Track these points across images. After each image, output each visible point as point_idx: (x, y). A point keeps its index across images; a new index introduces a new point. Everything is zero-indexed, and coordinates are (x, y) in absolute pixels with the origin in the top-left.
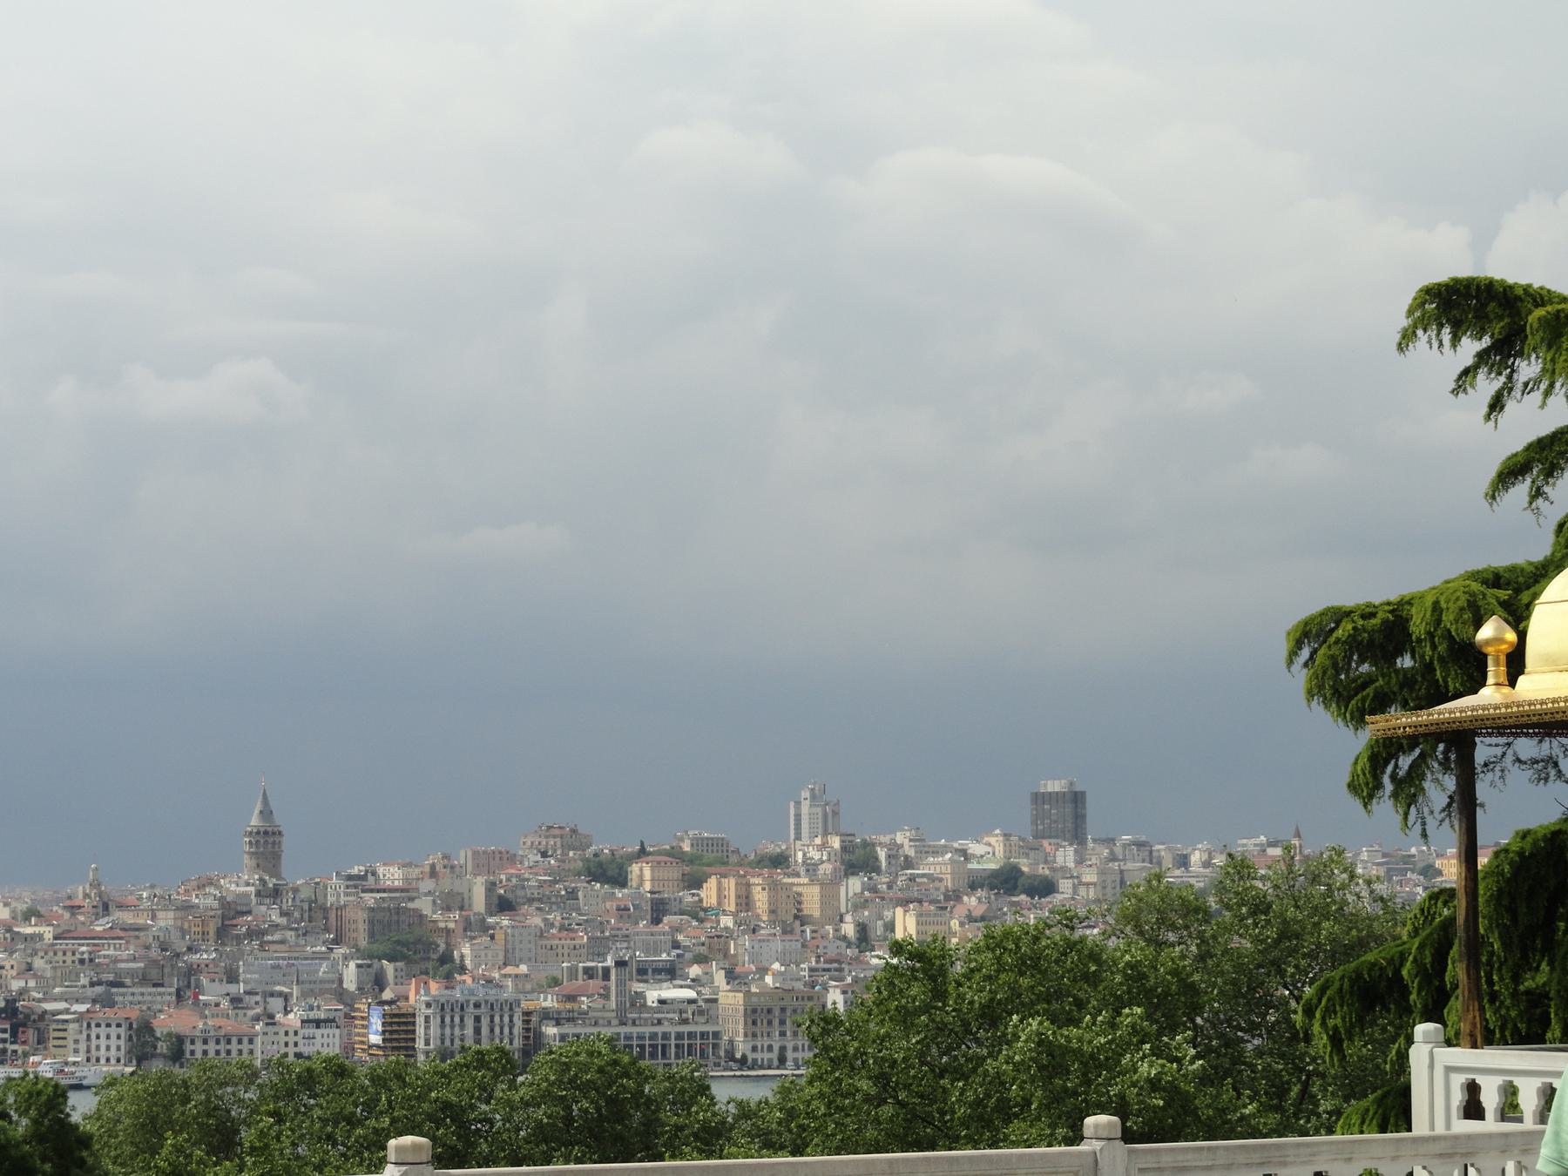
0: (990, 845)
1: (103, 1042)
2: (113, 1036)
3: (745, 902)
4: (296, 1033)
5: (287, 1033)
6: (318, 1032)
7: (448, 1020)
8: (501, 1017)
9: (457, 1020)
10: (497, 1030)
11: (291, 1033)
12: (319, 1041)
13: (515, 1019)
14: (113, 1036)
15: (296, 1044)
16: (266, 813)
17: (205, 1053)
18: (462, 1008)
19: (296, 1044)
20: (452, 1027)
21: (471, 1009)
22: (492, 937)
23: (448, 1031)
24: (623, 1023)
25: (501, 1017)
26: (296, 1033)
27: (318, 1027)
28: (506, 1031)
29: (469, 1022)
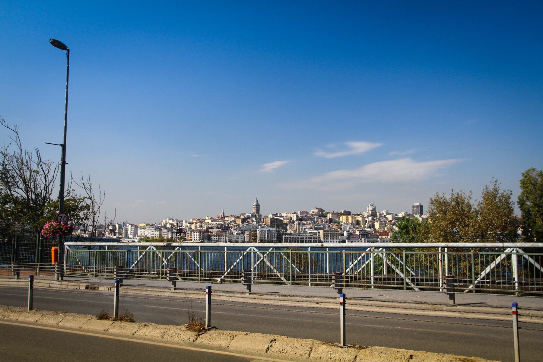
0: (402, 214)
1: (195, 236)
2: (197, 235)
3: (347, 220)
4: (235, 236)
5: (233, 236)
6: (240, 236)
7: (262, 234)
8: (273, 233)
9: (264, 234)
10: (272, 236)
11: (234, 236)
12: (240, 238)
13: (276, 234)
14: (197, 235)
15: (235, 238)
16: (257, 202)
17: (214, 239)
18: (265, 232)
19: (235, 238)
20: (263, 235)
21: (267, 232)
22: (294, 224)
23: (262, 236)
24: (299, 236)
25: (273, 233)
26: (235, 236)
27: (239, 235)
28: (274, 236)
29: (266, 234)
